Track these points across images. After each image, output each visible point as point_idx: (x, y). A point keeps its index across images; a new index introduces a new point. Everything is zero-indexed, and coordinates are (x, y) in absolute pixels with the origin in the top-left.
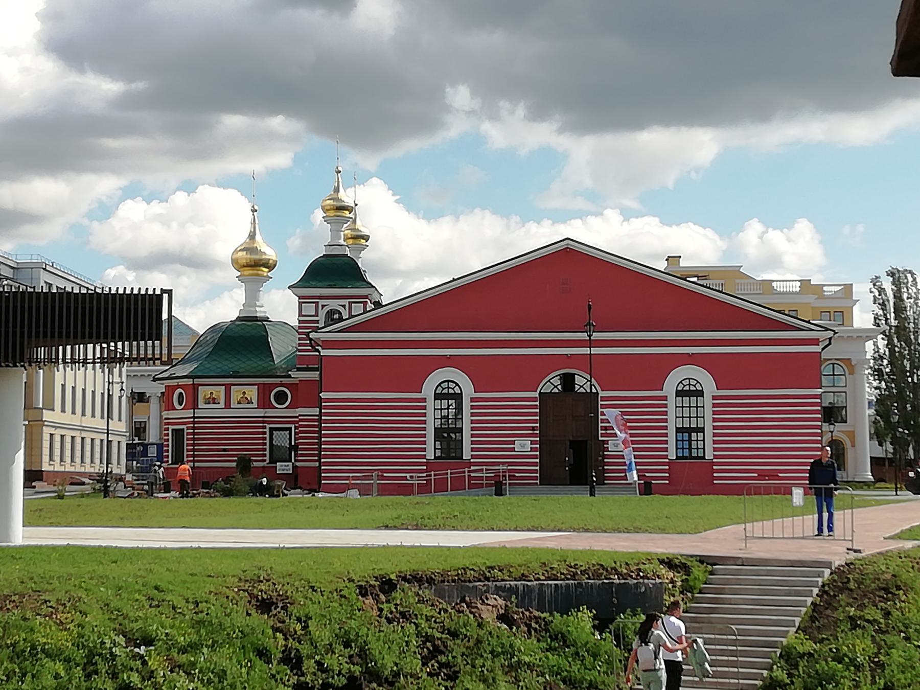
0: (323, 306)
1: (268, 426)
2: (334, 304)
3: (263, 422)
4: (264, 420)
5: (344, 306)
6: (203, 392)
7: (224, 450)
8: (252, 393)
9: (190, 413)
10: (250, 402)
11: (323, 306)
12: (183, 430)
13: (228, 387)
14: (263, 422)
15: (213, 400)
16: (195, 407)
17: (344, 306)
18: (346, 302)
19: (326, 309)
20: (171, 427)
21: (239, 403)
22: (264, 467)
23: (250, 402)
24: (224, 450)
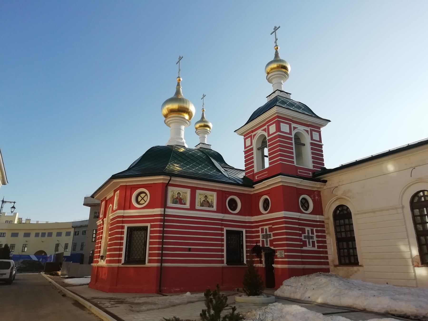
0: (295, 128)
1: (225, 229)
2: (301, 129)
3: (222, 225)
4: (222, 223)
5: (307, 131)
6: (172, 192)
7: (190, 250)
8: (213, 197)
9: (158, 211)
10: (211, 206)
11: (295, 128)
12: (146, 228)
13: (194, 190)
14: (222, 225)
15: (179, 200)
16: (164, 206)
17: (307, 131)
18: (308, 129)
19: (296, 131)
20: (126, 226)
21: (202, 205)
22: (223, 268)
23: (211, 206)
24: (190, 250)
